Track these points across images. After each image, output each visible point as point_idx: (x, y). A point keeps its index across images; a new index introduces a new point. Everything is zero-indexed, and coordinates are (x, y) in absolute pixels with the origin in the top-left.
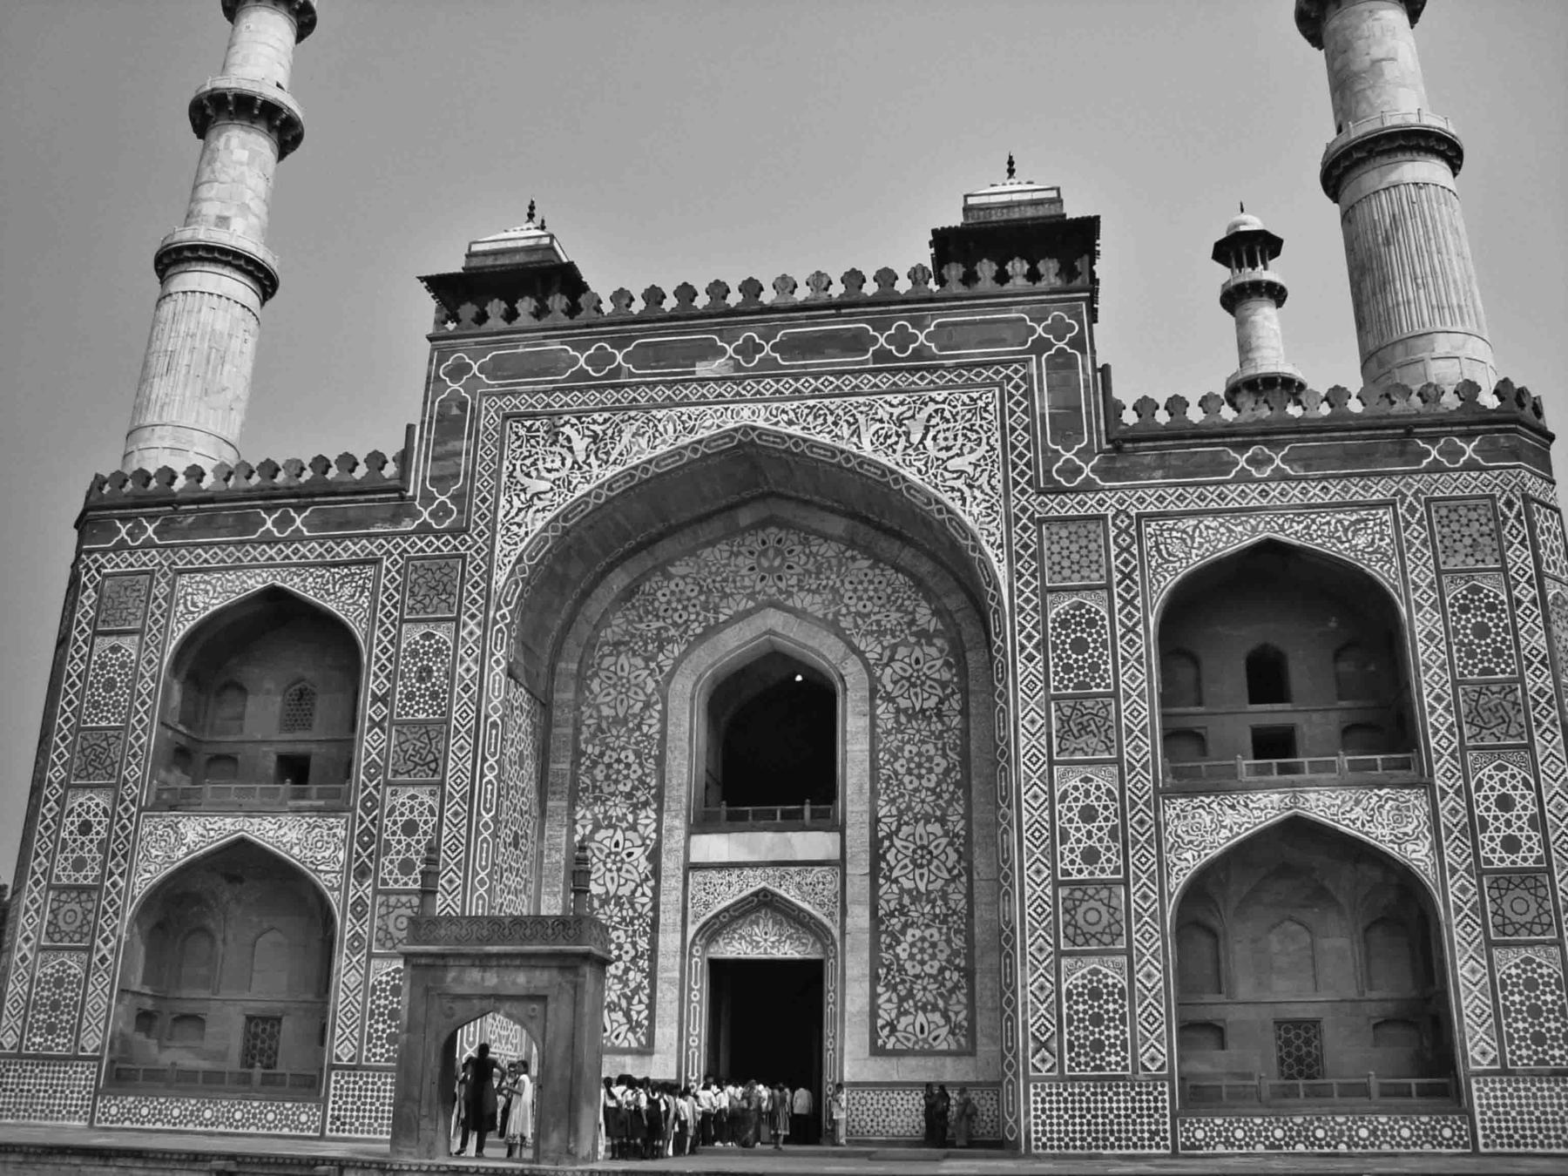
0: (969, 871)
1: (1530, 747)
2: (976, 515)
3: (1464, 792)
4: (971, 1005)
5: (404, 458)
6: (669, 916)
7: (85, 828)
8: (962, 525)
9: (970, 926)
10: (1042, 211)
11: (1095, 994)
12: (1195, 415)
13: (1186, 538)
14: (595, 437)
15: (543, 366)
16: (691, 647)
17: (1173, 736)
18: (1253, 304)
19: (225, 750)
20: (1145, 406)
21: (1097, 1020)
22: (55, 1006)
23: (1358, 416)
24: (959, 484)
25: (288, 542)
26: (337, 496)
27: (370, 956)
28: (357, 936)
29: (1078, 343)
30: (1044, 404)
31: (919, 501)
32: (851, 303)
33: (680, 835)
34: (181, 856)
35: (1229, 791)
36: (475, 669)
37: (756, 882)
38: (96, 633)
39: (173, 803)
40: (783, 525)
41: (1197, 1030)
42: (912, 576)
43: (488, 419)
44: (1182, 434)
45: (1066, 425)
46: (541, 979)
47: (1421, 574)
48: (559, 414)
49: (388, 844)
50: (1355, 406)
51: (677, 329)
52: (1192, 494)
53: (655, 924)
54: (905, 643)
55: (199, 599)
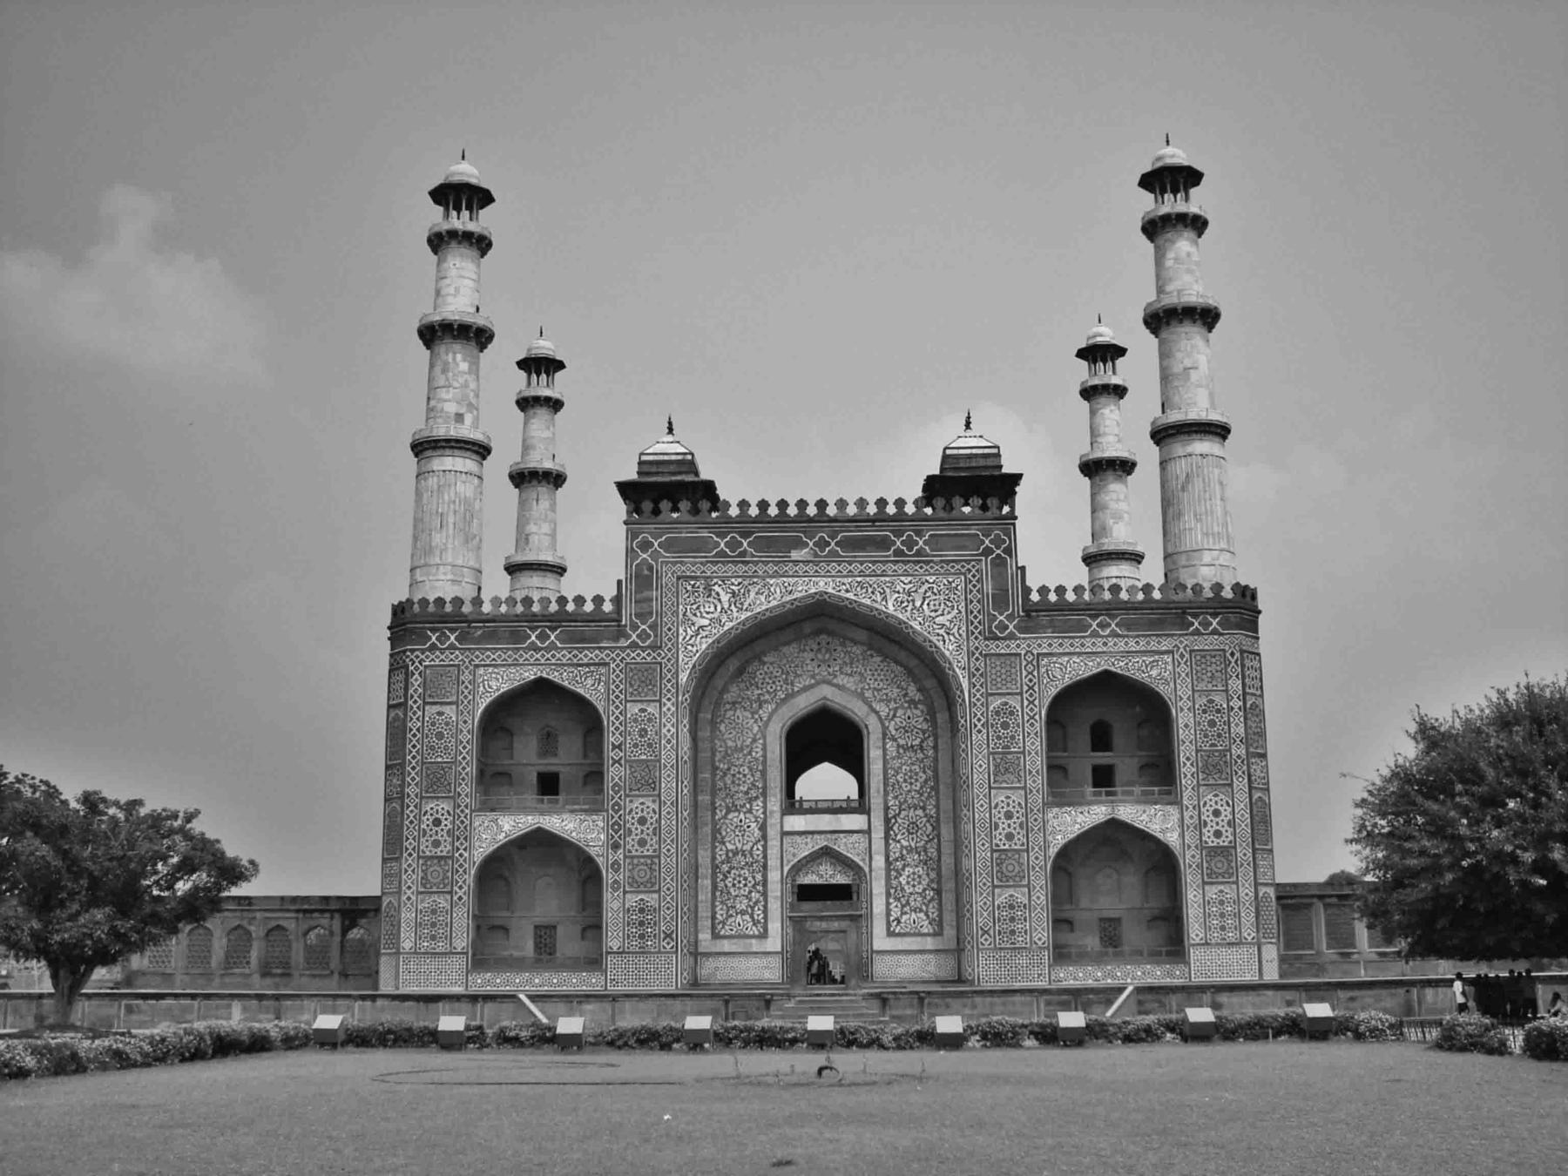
0: (939, 836)
1: (1231, 785)
2: (948, 649)
3: (1197, 807)
4: (940, 910)
5: (617, 600)
6: (773, 862)
7: (437, 822)
8: (943, 655)
9: (939, 867)
10: (990, 462)
11: (1012, 907)
12: (1070, 596)
13: (1063, 667)
14: (733, 593)
15: (698, 546)
16: (778, 706)
17: (1052, 767)
18: (1103, 400)
19: (500, 769)
20: (1043, 590)
21: (1012, 919)
22: (434, 925)
23: (1157, 601)
24: (941, 632)
25: (548, 649)
26: (581, 625)
27: (625, 892)
28: (616, 882)
29: (1008, 551)
30: (989, 588)
31: (919, 639)
32: (881, 518)
33: (778, 815)
34: (502, 838)
35: (1081, 804)
36: (673, 730)
37: (821, 842)
38: (425, 703)
39: (489, 806)
40: (831, 633)
41: (1061, 923)
42: (906, 668)
43: (668, 579)
44: (1062, 607)
45: (1001, 600)
46: (844, 924)
47: (1184, 691)
48: (711, 578)
49: (630, 831)
50: (1157, 595)
51: (780, 530)
52: (1067, 642)
53: (765, 866)
54: (902, 707)
55: (494, 684)
